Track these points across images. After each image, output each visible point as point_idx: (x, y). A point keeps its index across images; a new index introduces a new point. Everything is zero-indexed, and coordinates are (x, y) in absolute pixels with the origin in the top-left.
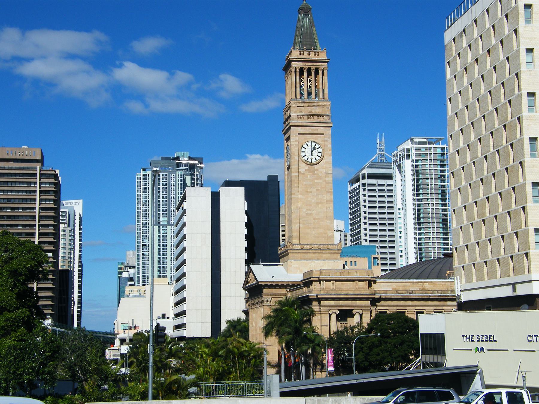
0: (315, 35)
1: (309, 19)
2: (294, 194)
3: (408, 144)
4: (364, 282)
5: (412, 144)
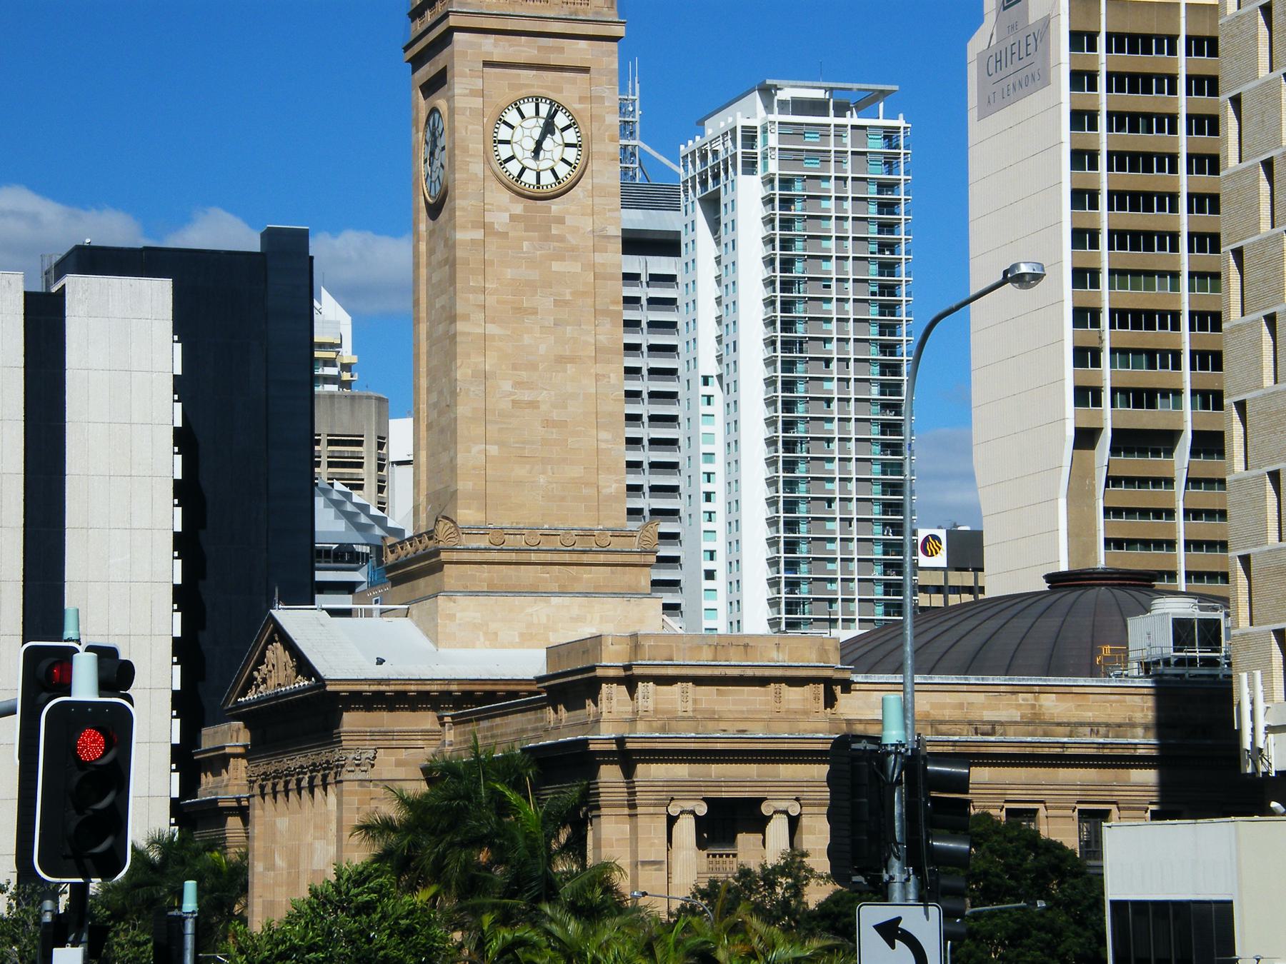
2: (466, 318)
3: (750, 112)
4: (808, 690)
5: (768, 108)
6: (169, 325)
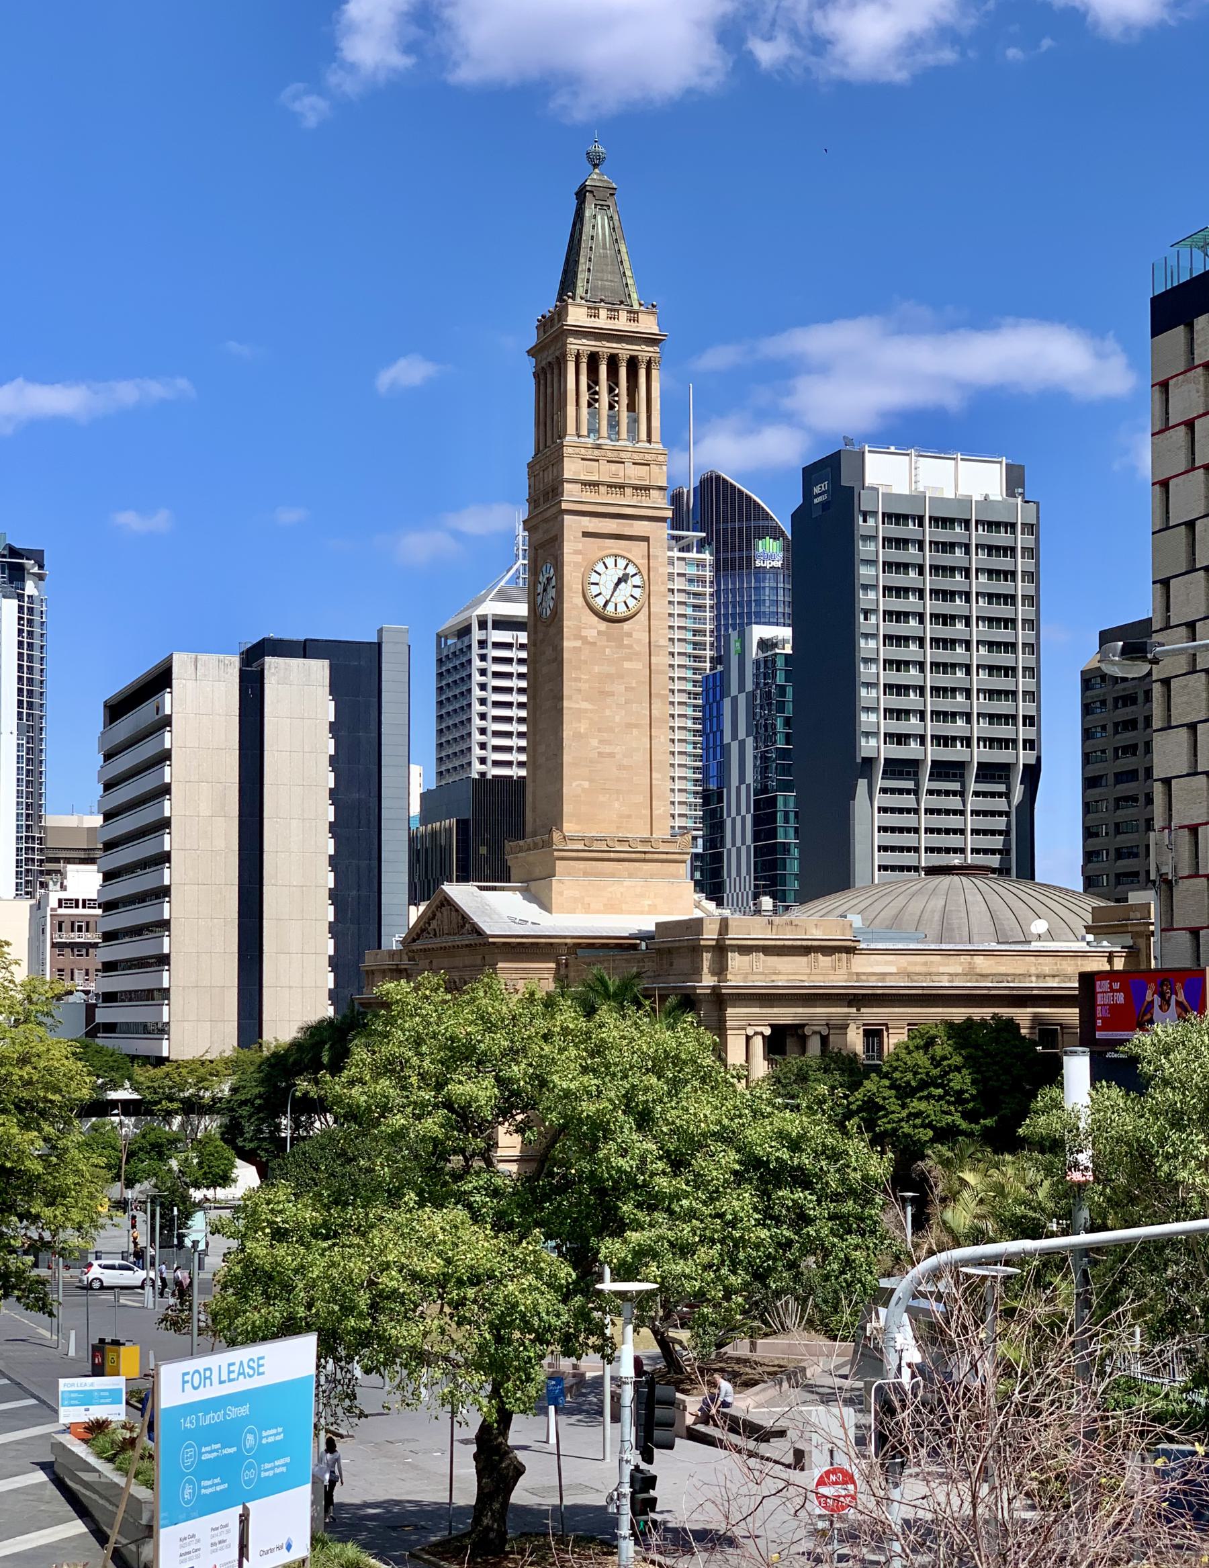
0: (627, 265)
1: (611, 219)
2: (570, 698)
6: (327, 689)
